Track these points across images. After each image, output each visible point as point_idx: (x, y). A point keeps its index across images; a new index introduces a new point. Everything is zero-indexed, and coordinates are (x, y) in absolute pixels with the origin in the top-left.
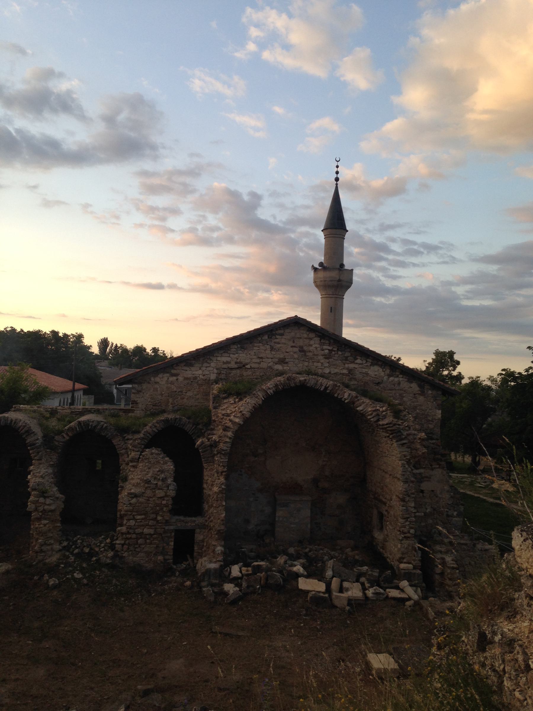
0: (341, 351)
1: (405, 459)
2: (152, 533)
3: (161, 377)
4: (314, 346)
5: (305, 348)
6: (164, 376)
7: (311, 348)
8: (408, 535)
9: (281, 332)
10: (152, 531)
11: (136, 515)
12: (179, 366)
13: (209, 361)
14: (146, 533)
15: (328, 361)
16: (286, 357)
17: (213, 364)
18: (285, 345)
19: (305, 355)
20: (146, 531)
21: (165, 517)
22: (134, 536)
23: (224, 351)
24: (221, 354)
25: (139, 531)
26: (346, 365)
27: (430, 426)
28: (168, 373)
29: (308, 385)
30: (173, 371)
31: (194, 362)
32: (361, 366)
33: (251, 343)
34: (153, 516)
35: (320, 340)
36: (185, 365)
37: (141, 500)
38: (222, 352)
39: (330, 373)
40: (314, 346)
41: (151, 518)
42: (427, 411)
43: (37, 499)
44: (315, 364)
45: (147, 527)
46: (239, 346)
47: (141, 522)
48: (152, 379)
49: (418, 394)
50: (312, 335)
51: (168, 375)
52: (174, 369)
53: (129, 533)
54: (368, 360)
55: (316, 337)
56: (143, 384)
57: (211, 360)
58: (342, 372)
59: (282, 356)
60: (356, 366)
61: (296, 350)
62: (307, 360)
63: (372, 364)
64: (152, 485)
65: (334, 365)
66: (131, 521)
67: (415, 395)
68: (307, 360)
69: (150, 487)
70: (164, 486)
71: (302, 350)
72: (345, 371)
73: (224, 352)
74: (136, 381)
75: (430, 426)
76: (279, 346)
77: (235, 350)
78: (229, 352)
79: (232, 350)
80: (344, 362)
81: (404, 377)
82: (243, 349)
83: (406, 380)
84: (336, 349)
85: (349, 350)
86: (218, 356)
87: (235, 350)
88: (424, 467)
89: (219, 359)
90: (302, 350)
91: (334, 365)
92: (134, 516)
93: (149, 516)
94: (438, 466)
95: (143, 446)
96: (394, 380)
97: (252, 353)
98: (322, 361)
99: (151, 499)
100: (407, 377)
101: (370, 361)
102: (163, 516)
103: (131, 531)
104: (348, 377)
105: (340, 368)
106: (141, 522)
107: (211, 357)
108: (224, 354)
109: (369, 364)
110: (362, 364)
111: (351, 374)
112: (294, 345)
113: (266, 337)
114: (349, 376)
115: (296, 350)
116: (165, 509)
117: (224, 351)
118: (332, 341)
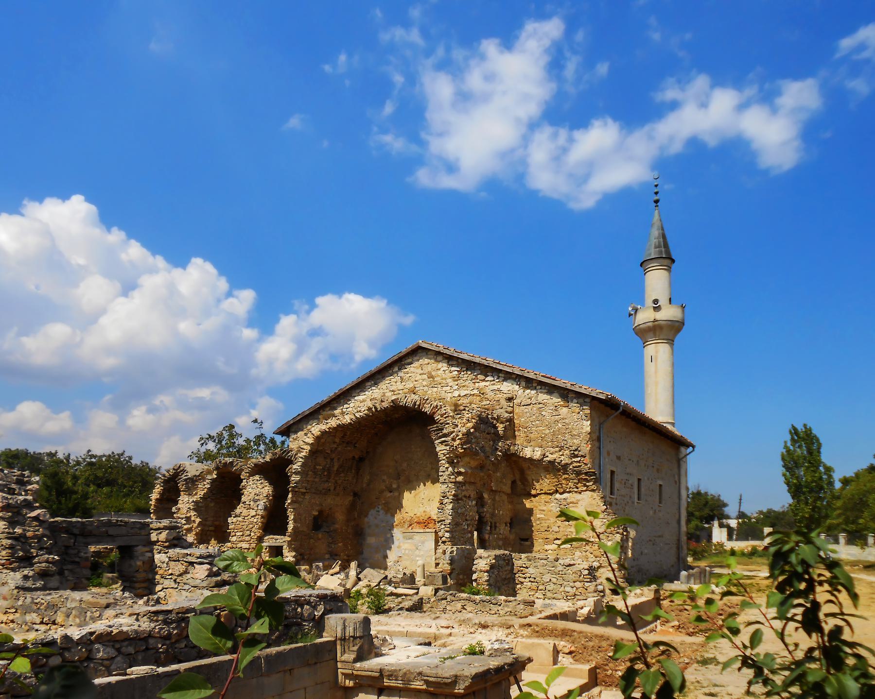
0: (471, 371)
1: (444, 458)
4: (442, 369)
5: (433, 373)
7: (439, 372)
8: (444, 539)
9: (410, 360)
10: (247, 546)
15: (456, 383)
16: (416, 386)
17: (352, 405)
18: (414, 374)
19: (434, 381)
25: (239, 545)
26: (477, 384)
27: (575, 441)
29: (401, 404)
32: (492, 383)
34: (248, 533)
35: (448, 362)
37: (240, 519)
38: (358, 391)
39: (459, 396)
40: (442, 369)
42: (572, 424)
44: (444, 389)
46: (373, 382)
49: (561, 405)
50: (440, 358)
54: (500, 375)
55: (443, 359)
58: (472, 393)
59: (411, 385)
60: (487, 384)
61: (425, 377)
62: (435, 386)
63: (505, 380)
65: (464, 386)
67: (556, 407)
68: (435, 386)
71: (431, 376)
72: (476, 392)
75: (575, 441)
76: (409, 375)
80: (474, 381)
81: (543, 387)
83: (545, 391)
84: (465, 369)
85: (479, 368)
88: (568, 490)
89: (356, 398)
90: (431, 376)
91: (464, 386)
94: (585, 488)
96: (530, 393)
97: (384, 387)
98: (450, 385)
99: (246, 518)
100: (547, 388)
101: (503, 375)
104: (478, 398)
105: (470, 389)
109: (501, 379)
110: (494, 380)
111: (483, 394)
112: (422, 372)
113: (396, 369)
114: (480, 396)
115: (425, 377)
118: (460, 361)
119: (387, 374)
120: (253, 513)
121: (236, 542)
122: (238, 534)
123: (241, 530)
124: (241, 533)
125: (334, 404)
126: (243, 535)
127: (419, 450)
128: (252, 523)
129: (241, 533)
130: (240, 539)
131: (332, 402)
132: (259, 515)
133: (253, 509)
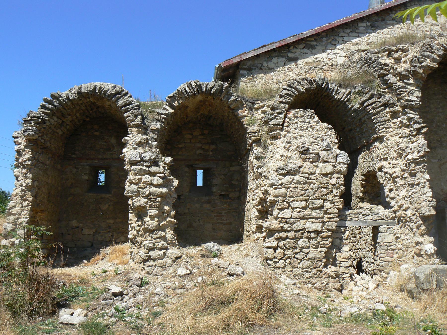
2: (320, 229)
3: (276, 61)
6: (279, 60)
10: (318, 227)
11: (292, 201)
12: (296, 48)
13: (333, 43)
14: (311, 230)
20: (311, 225)
21: (336, 204)
22: (291, 234)
23: (351, 30)
24: (348, 33)
25: (300, 224)
28: (283, 57)
30: (290, 55)
31: (315, 43)
33: (383, 20)
34: (319, 202)
36: (304, 48)
37: (297, 178)
38: (348, 31)
41: (315, 206)
43: (139, 177)
45: (310, 220)
46: (369, 24)
47: (300, 212)
48: (265, 64)
51: (284, 59)
52: (292, 52)
53: (282, 230)
56: (253, 71)
57: (336, 40)
64: (312, 156)
66: (285, 210)
69: (309, 158)
70: (330, 157)
73: (351, 31)
74: (244, 67)
77: (364, 28)
78: (357, 31)
79: (361, 28)
82: (373, 27)
86: (345, 36)
87: (364, 28)
92: (288, 203)
93: (313, 203)
95: (287, 106)
102: (334, 202)
103: (286, 226)
106: (300, 212)
107: (336, 38)
108: (351, 34)
116: (335, 191)
117: (351, 30)
119: (387, 17)
120: (329, 168)
121: (292, 220)
122: (295, 205)
123: (302, 197)
124: (303, 204)
125: (310, 41)
126: (305, 208)
127: (440, 110)
128: (325, 185)
129: (303, 204)
130: (302, 214)
131: (309, 39)
132: (338, 172)
133: (326, 162)
